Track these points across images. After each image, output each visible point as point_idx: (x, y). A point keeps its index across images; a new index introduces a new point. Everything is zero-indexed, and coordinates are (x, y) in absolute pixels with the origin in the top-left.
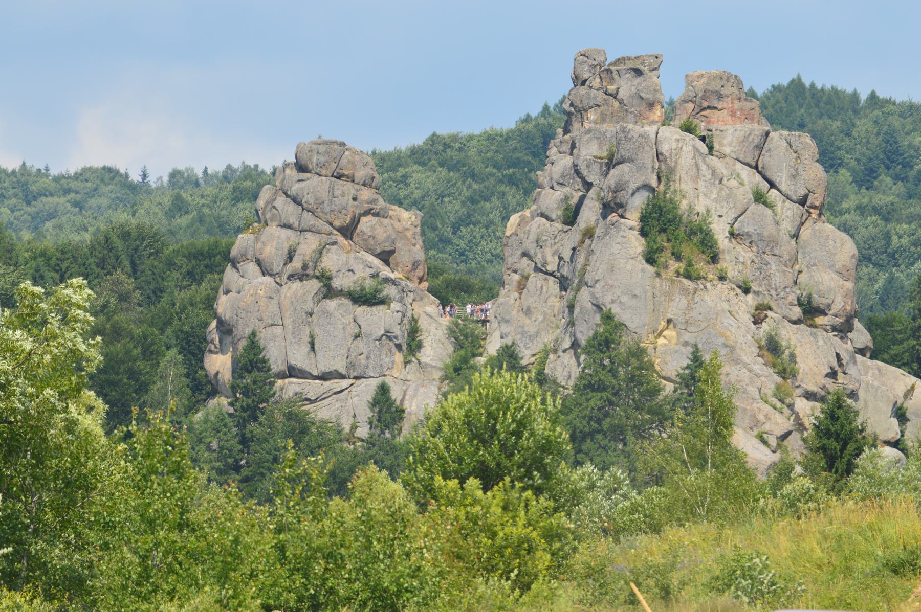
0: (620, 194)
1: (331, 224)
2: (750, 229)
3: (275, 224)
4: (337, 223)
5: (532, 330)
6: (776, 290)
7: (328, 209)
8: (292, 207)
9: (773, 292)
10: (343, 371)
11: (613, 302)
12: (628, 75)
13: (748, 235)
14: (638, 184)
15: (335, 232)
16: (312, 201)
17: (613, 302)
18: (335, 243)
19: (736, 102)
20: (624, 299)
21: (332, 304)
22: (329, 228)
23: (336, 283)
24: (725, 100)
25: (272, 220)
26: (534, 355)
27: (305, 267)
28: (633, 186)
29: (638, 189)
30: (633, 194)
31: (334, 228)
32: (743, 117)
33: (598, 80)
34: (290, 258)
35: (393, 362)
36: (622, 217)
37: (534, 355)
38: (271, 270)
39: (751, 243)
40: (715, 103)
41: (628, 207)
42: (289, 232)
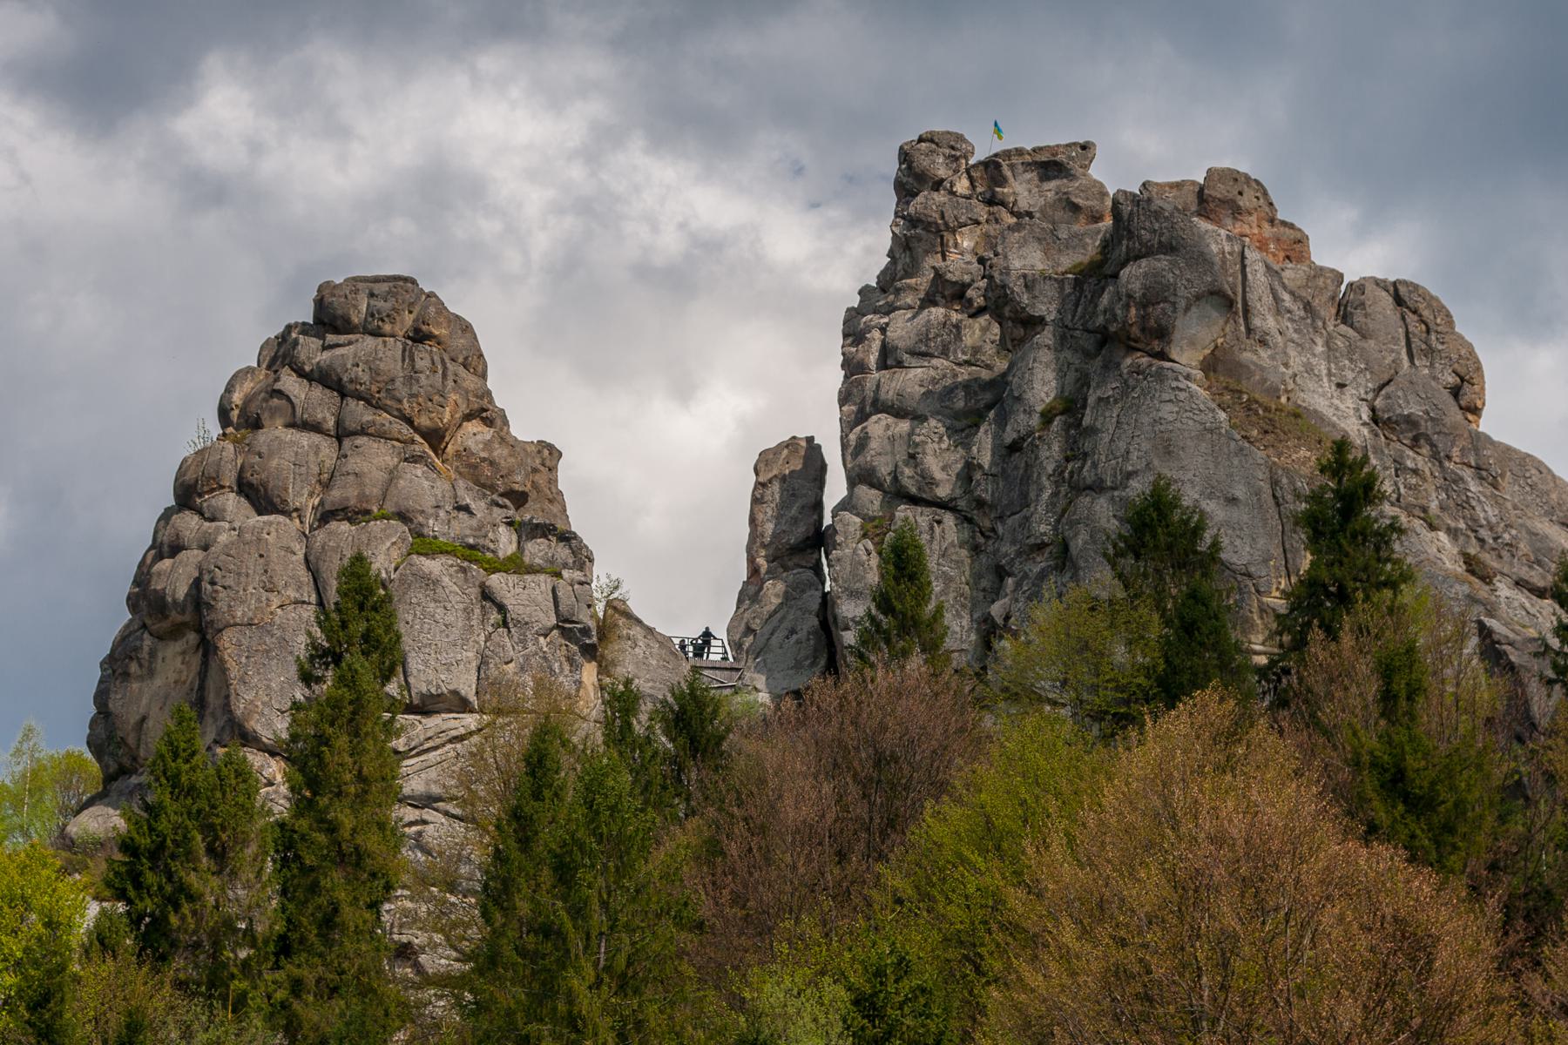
2: (1414, 409)
3: (279, 422)
4: (423, 421)
6: (1491, 529)
7: (402, 390)
8: (318, 392)
9: (1484, 533)
10: (469, 691)
12: (1028, 176)
13: (1411, 421)
15: (418, 438)
16: (365, 378)
19: (1266, 225)
22: (406, 431)
23: (434, 526)
24: (1246, 218)
25: (274, 412)
29: (1198, 298)
30: (1187, 309)
31: (417, 430)
32: (1282, 255)
33: (965, 182)
34: (326, 486)
35: (579, 683)
36: (1163, 356)
38: (284, 501)
39: (1416, 439)
41: (1176, 336)
42: (316, 438)
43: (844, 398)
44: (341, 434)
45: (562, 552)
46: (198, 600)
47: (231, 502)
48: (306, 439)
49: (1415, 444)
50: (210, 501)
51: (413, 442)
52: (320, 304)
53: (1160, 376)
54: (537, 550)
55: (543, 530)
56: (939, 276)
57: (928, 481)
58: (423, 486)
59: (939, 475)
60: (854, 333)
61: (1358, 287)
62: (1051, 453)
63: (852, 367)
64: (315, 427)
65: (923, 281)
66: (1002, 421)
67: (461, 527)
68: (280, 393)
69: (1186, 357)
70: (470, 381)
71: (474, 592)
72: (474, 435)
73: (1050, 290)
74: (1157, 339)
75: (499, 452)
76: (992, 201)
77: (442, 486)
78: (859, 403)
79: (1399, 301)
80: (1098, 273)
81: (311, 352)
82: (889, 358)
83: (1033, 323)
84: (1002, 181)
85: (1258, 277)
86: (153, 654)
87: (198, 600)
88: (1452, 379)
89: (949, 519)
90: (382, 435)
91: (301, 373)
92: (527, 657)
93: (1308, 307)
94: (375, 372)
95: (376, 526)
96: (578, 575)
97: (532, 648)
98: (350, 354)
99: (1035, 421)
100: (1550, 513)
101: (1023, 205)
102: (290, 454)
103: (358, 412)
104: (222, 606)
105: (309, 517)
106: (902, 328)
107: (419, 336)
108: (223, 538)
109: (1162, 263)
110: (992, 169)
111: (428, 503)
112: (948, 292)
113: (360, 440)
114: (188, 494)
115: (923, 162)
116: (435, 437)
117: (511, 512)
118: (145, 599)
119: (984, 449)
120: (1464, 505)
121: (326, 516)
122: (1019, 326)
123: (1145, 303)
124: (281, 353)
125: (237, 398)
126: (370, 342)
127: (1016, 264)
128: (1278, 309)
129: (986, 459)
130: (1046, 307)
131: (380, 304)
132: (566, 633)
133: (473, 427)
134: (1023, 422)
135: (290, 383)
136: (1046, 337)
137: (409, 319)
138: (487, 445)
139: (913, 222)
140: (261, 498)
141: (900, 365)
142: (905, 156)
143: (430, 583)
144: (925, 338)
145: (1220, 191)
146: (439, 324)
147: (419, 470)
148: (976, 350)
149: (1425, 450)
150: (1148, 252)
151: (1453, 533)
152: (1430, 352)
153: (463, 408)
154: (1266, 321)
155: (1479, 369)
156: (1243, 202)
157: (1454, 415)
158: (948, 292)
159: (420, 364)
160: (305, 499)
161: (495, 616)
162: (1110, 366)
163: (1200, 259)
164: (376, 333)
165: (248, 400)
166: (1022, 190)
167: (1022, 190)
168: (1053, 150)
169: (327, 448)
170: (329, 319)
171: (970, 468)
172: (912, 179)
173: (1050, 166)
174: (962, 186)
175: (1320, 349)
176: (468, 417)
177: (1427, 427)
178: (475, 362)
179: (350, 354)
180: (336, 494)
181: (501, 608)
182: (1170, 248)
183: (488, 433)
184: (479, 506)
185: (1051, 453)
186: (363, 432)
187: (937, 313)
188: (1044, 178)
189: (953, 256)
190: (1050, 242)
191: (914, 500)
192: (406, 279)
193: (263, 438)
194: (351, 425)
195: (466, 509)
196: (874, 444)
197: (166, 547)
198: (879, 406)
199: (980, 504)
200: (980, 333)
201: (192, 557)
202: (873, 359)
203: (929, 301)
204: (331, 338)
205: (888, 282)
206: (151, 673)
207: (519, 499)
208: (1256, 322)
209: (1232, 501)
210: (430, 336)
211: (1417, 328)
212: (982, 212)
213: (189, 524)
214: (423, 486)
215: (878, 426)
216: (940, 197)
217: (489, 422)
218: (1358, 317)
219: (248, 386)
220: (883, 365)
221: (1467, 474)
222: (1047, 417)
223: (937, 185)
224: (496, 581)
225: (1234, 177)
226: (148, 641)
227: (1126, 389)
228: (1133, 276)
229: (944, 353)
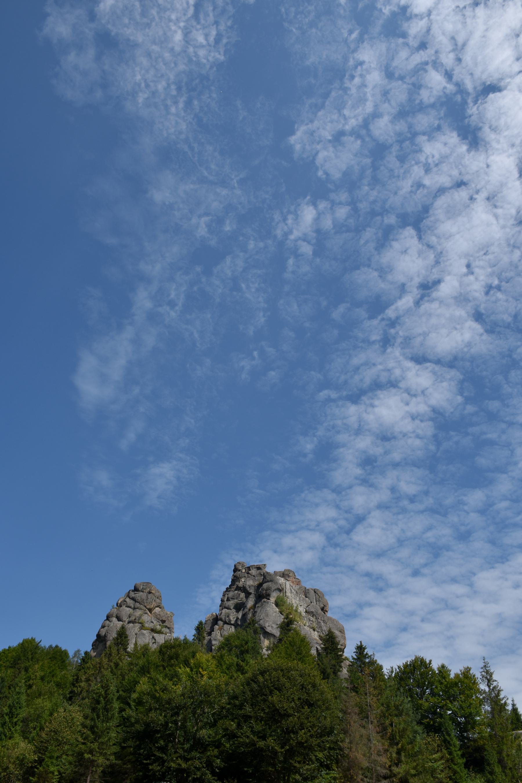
0: (268, 592)
2: (313, 610)
4: (148, 607)
7: (145, 601)
8: (132, 601)
9: (324, 632)
11: (269, 626)
13: (312, 612)
14: (276, 588)
16: (140, 599)
17: (269, 626)
18: (146, 613)
21: (145, 632)
22: (145, 608)
23: (146, 625)
25: (124, 604)
27: (135, 619)
28: (273, 589)
29: (275, 589)
34: (130, 617)
41: (271, 596)
42: (130, 609)
43: (220, 606)
44: (134, 609)
45: (168, 630)
46: (105, 636)
47: (114, 619)
48: (128, 609)
49: (313, 616)
50: (111, 619)
52: (135, 587)
53: (268, 603)
54: (165, 630)
55: (166, 627)
56: (237, 586)
57: (230, 621)
58: (146, 618)
59: (232, 619)
60: (224, 595)
61: (308, 590)
62: (250, 615)
63: (222, 601)
64: (130, 607)
65: (235, 587)
66: (243, 610)
67: (151, 626)
68: (125, 601)
69: (272, 600)
70: (158, 600)
71: (151, 637)
72: (157, 610)
73: (253, 588)
74: (268, 596)
75: (162, 613)
76: (248, 573)
77: (150, 618)
78: (223, 606)
79: (315, 592)
80: (260, 585)
81: (132, 594)
82: (228, 600)
83: (250, 594)
84: (250, 570)
85: (288, 586)
86: (98, 645)
87: (105, 636)
88: (322, 606)
89: (233, 627)
90: (141, 609)
91: (130, 598)
93: (296, 592)
94: (141, 598)
95: (137, 624)
96: (170, 635)
98: (138, 595)
99: (248, 610)
100: (337, 629)
101: (253, 574)
102: (126, 611)
103: (138, 605)
104: (108, 637)
105: (126, 622)
106: (231, 594)
107: (150, 593)
108: (112, 625)
109: (270, 583)
110: (249, 568)
111: (146, 620)
112: (238, 588)
113: (137, 610)
114: (108, 618)
115: (237, 567)
116: (150, 610)
117: (161, 623)
118: (98, 636)
119: (240, 615)
120: (321, 627)
121: (129, 622)
122: (248, 594)
123: (266, 590)
124: (128, 596)
125: (119, 602)
126: (141, 593)
127: (248, 583)
128: (291, 592)
129: (240, 617)
130: (252, 591)
131: (144, 587)
133: (157, 609)
134: (246, 610)
135: (128, 600)
136: (252, 596)
137: (148, 589)
138: (159, 612)
139: (234, 576)
140: (119, 619)
141: (229, 600)
142: (235, 566)
143: (144, 634)
144: (234, 596)
145: (286, 573)
147: (146, 615)
148: (242, 598)
149: (315, 617)
150: (268, 581)
151: (318, 632)
152: (319, 601)
153: (156, 605)
154: (288, 594)
155: (328, 604)
157: (320, 611)
158: (238, 588)
160: (126, 619)
161: (154, 641)
162: (261, 600)
163: (276, 583)
164: (143, 592)
165: (121, 602)
166: (253, 572)
167: (253, 572)
168: (260, 565)
169: (131, 610)
170: (136, 589)
171: (238, 618)
172: (236, 570)
173: (259, 568)
174: (244, 571)
175: (298, 599)
176: (157, 607)
177: (315, 613)
178: (159, 597)
179: (138, 595)
180: (131, 619)
181: (155, 640)
182: (271, 581)
183: (160, 610)
184: (155, 622)
185: (250, 615)
186: (138, 608)
187: (236, 592)
188: (258, 570)
189: (241, 583)
190: (254, 580)
191: (228, 624)
193: (121, 608)
194: (136, 607)
195: (153, 622)
196: (223, 614)
197: (103, 627)
198: (225, 608)
199: (238, 624)
200: (243, 595)
201: (106, 628)
202: (226, 599)
203: (236, 590)
204: (136, 592)
205: (230, 586)
206: (97, 648)
207: (163, 622)
208: (287, 594)
211: (318, 597)
212: (246, 575)
213: (108, 622)
214: (146, 618)
215: (225, 611)
216: (239, 572)
217: (160, 608)
218: (308, 595)
219: (122, 600)
220: (227, 601)
221: (322, 622)
222: (249, 610)
223: (239, 570)
224: (156, 635)
225: (289, 570)
226: (98, 643)
227: (262, 605)
228: (265, 586)
229: (237, 599)
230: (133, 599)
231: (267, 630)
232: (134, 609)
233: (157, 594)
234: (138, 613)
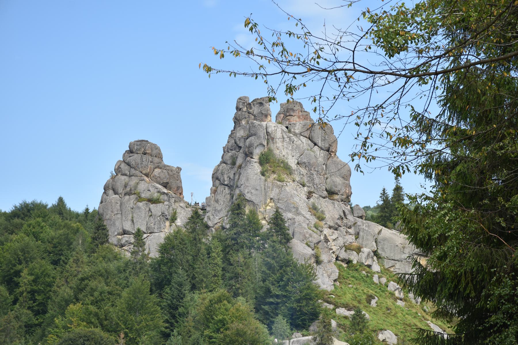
0: (251, 149)
1: (141, 172)
2: (305, 161)
4: (144, 172)
5: (219, 208)
7: (140, 166)
8: (127, 167)
9: (315, 186)
11: (248, 192)
13: (304, 163)
15: (143, 176)
16: (134, 164)
17: (248, 192)
18: (143, 180)
19: (300, 113)
20: (253, 191)
21: (140, 204)
22: (141, 174)
23: (143, 195)
26: (220, 219)
27: (131, 190)
28: (255, 145)
29: (258, 145)
30: (256, 148)
33: (246, 108)
34: (125, 187)
36: (252, 158)
37: (220, 219)
40: (292, 114)
41: (254, 154)
42: (125, 177)
48: (123, 177)
51: (142, 176)
64: (126, 175)
70: (156, 160)
71: (148, 209)
89: (227, 188)
92: (155, 222)
97: (156, 220)
103: (133, 171)
105: (123, 195)
111: (143, 189)
113: (133, 177)
126: (136, 155)
132: (163, 216)
133: (156, 170)
137: (143, 150)
138: (159, 174)
143: (139, 208)
146: (148, 150)
149: (307, 169)
156: (295, 108)
159: (144, 160)
176: (156, 168)
177: (307, 164)
192: (143, 141)
195: (149, 190)
209: (257, 190)
210: (147, 153)
221: (315, 173)
224: (152, 206)
230: (128, 164)
231: (246, 198)
232: (130, 176)
233: (155, 152)
234: (133, 181)
